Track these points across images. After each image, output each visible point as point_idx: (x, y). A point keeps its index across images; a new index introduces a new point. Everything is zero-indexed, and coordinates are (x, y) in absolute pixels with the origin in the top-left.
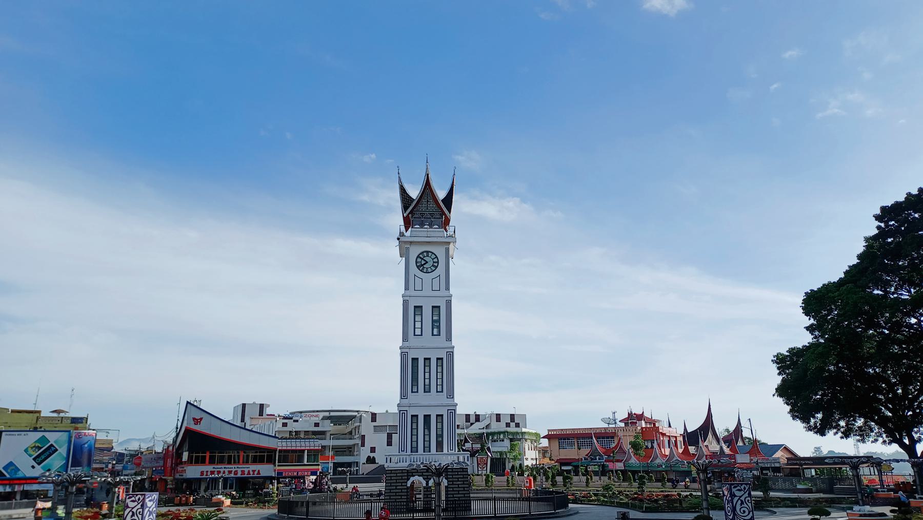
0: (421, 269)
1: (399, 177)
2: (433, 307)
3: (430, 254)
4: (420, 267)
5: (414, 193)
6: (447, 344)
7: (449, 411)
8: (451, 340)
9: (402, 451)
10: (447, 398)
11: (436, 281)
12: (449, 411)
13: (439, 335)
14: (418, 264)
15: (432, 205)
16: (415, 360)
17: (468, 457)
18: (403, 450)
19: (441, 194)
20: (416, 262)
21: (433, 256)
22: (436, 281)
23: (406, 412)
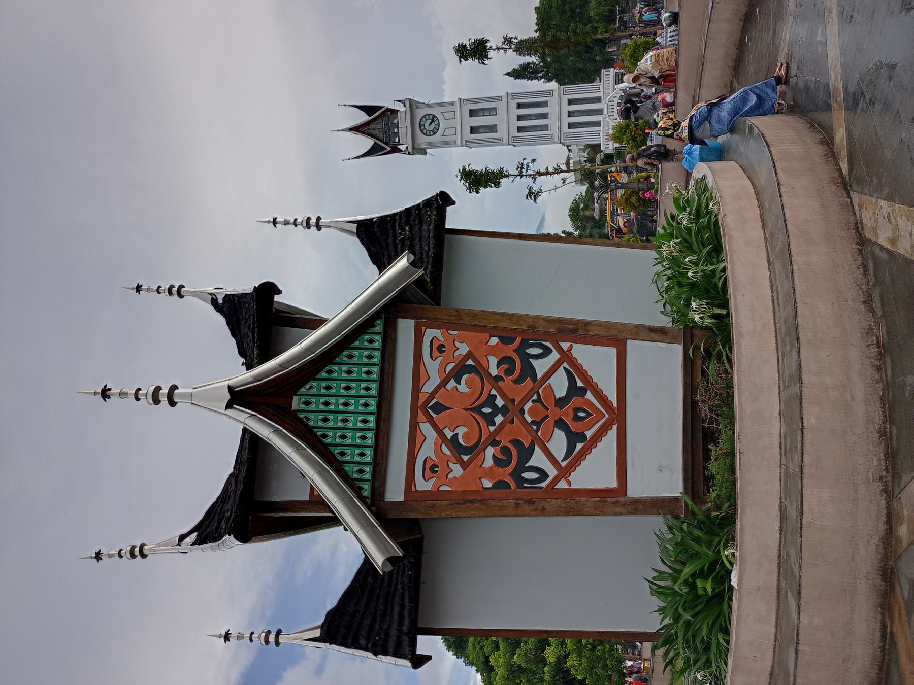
0: (436, 131)
1: (353, 159)
2: (471, 116)
3: (422, 123)
4: (434, 132)
5: (368, 143)
6: (504, 100)
7: (565, 93)
8: (501, 97)
9: (599, 135)
10: (552, 96)
11: (447, 115)
12: (565, 93)
13: (495, 108)
14: (432, 134)
15: (378, 125)
16: (520, 129)
17: (606, 71)
18: (598, 134)
19: (364, 118)
20: (430, 135)
21: (424, 120)
22: (447, 115)
23: (565, 135)
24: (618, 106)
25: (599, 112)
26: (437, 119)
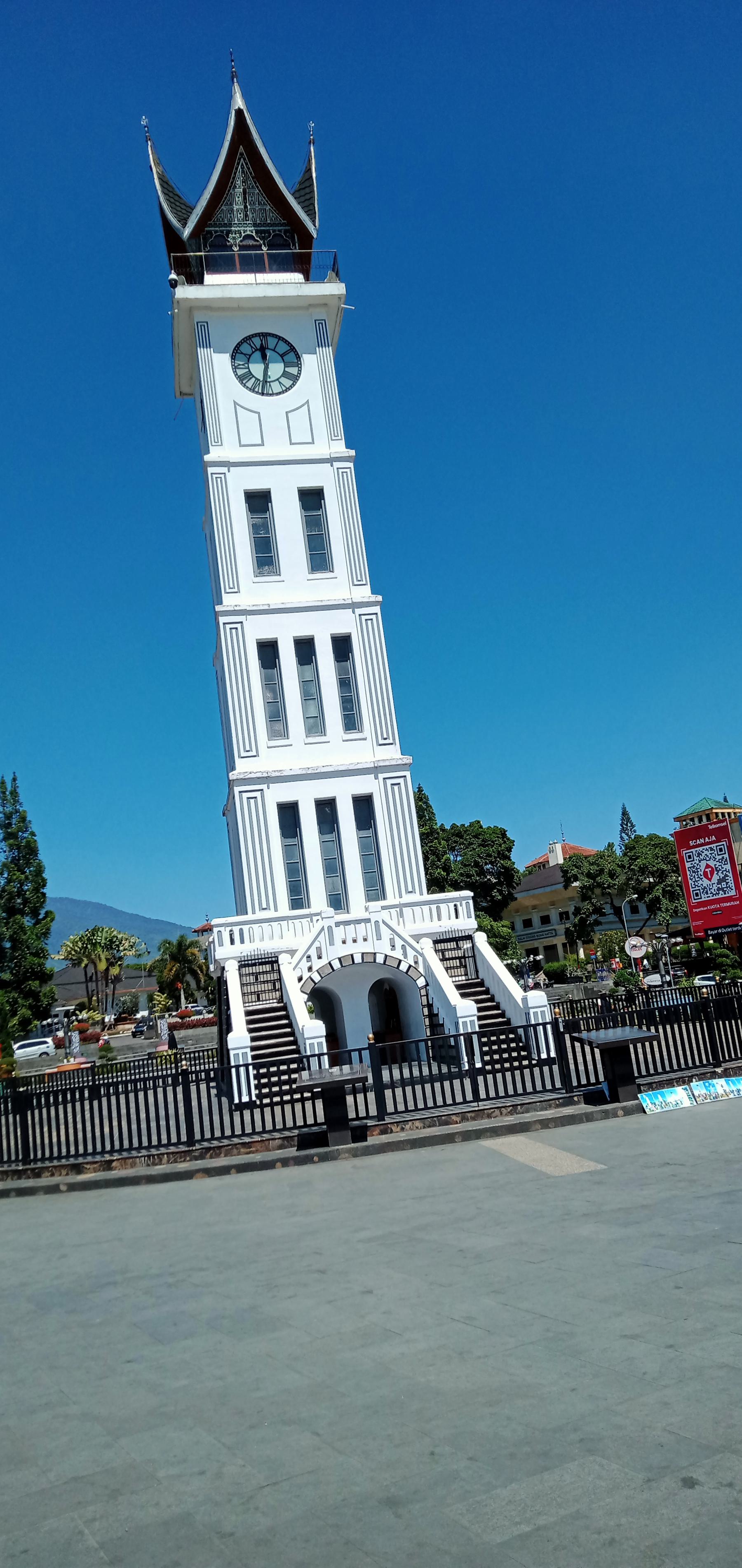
0: (250, 384)
11: (299, 420)
21: (282, 348)
22: (299, 420)
24: (363, 954)
25: (338, 901)
26: (288, 389)
